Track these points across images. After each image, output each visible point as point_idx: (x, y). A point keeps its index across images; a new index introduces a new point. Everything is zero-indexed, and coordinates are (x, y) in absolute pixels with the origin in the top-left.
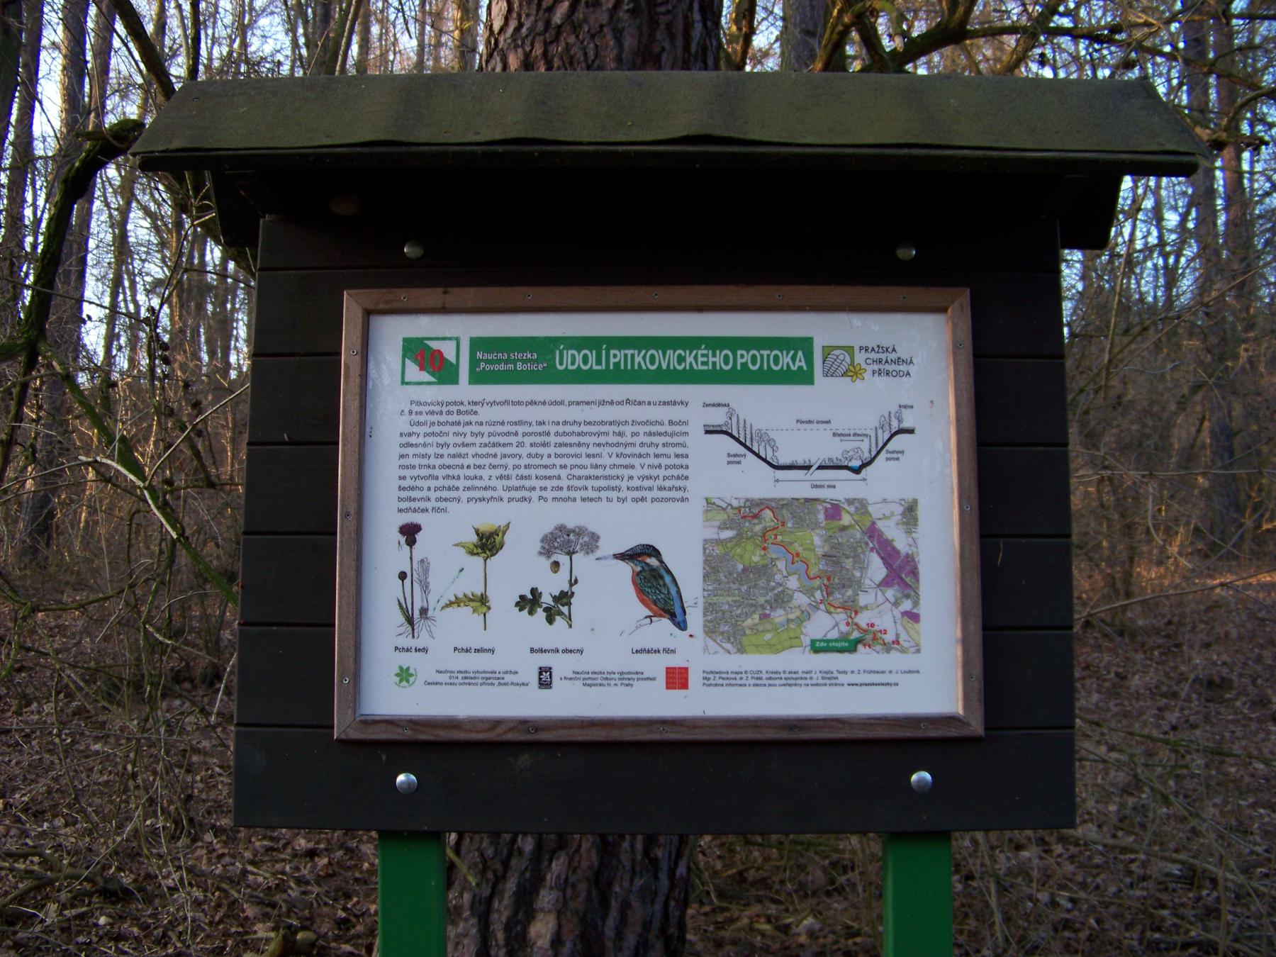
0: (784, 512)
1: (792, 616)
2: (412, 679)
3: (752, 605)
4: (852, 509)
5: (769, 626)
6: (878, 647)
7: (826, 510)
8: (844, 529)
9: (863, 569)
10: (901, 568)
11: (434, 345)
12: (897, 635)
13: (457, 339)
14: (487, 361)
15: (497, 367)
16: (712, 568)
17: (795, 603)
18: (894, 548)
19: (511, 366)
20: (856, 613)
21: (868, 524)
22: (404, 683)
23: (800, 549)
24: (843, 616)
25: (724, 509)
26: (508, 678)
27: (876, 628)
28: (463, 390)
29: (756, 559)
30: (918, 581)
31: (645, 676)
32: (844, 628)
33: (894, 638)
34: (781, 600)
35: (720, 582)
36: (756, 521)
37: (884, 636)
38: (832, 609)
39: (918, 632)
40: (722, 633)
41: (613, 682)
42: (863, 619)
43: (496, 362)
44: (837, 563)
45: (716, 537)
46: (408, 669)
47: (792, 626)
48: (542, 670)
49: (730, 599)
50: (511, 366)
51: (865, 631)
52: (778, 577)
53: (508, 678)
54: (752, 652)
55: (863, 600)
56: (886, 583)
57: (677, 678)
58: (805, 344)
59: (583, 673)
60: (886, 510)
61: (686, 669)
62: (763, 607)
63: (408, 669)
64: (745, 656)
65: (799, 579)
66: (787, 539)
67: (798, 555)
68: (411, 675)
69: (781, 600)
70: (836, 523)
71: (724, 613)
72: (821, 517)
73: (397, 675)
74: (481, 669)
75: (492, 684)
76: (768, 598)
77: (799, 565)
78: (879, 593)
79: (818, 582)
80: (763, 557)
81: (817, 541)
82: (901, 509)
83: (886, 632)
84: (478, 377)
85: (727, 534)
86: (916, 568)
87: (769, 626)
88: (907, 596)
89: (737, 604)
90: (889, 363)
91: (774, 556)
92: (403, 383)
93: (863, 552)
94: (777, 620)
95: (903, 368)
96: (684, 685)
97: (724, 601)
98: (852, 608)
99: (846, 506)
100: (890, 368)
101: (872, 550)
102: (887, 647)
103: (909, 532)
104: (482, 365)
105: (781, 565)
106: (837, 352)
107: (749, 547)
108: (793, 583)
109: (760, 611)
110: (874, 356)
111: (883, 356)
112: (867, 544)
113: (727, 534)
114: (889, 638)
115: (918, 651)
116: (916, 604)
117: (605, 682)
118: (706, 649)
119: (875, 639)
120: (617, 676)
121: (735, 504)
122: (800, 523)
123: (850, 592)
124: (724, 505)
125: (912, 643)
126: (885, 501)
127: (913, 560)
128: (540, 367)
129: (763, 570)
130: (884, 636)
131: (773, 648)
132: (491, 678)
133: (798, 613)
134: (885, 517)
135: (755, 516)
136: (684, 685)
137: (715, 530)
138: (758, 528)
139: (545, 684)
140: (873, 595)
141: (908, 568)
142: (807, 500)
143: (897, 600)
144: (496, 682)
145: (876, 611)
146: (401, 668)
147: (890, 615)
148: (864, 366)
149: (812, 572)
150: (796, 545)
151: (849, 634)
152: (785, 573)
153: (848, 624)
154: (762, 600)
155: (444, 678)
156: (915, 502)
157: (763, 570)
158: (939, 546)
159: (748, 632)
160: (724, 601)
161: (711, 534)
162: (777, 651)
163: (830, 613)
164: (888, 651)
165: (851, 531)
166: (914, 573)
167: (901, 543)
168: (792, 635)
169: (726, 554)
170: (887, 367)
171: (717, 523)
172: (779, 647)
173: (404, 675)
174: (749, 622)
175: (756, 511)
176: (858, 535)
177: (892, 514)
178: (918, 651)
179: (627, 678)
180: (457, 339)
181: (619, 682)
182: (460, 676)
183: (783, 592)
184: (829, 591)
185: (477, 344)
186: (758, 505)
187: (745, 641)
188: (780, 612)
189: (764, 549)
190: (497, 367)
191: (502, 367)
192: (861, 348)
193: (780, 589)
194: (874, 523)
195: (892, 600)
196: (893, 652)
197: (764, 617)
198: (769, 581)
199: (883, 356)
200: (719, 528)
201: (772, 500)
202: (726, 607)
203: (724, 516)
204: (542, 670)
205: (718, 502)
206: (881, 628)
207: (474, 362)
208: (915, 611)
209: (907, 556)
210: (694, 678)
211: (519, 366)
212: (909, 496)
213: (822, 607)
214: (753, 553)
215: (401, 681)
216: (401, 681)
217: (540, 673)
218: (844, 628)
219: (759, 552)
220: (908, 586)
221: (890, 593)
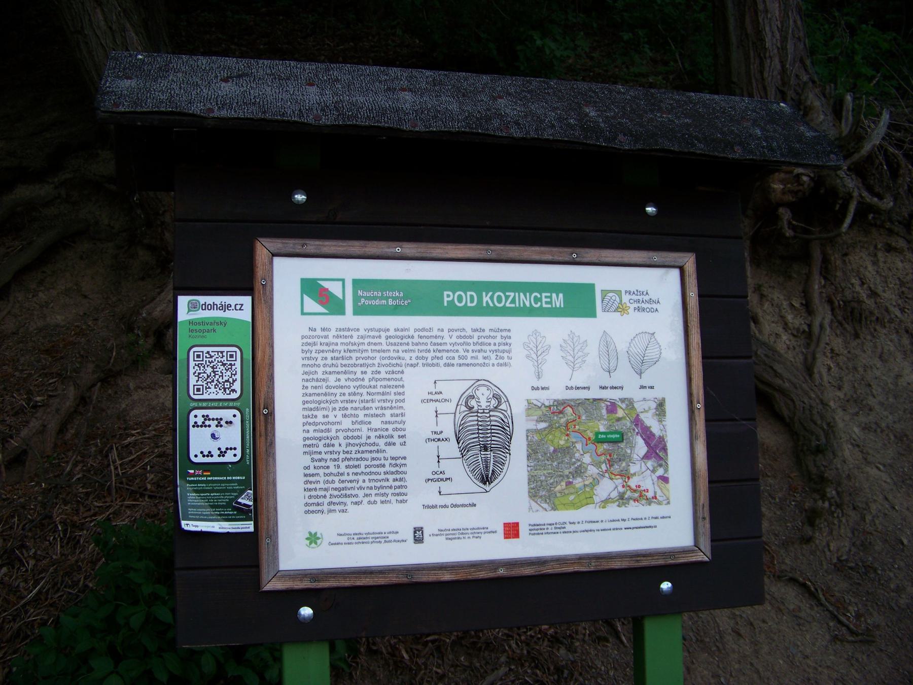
0: (580, 408)
1: (587, 483)
2: (319, 542)
3: (561, 476)
4: (624, 406)
5: (572, 490)
7: (607, 406)
8: (619, 420)
9: (632, 448)
10: (656, 446)
11: (325, 284)
12: (655, 493)
13: (343, 280)
14: (366, 298)
15: (374, 302)
17: (589, 473)
19: (384, 302)
20: (629, 478)
21: (634, 416)
22: (313, 545)
24: (620, 481)
25: (540, 408)
26: (392, 537)
28: (349, 319)
29: (562, 442)
30: (667, 454)
31: (489, 530)
32: (621, 489)
34: (579, 471)
36: (561, 415)
39: (668, 490)
40: (541, 497)
41: (467, 536)
42: (633, 483)
43: (374, 299)
45: (535, 427)
46: (316, 533)
48: (416, 530)
49: (545, 472)
50: (384, 302)
51: (635, 491)
52: (577, 455)
53: (392, 537)
55: (633, 469)
56: (646, 457)
57: (512, 531)
58: (589, 289)
59: (445, 530)
60: (646, 405)
61: (517, 524)
62: (568, 477)
63: (316, 533)
64: (557, 512)
65: (591, 456)
68: (319, 538)
69: (579, 471)
70: (614, 416)
71: (542, 482)
72: (604, 411)
73: (307, 539)
74: (371, 531)
75: (380, 542)
76: (571, 470)
79: (603, 458)
82: (654, 405)
84: (359, 310)
85: (543, 425)
87: (572, 490)
88: (661, 466)
89: (550, 475)
90: (646, 303)
91: (574, 440)
92: (303, 313)
94: (577, 486)
95: (655, 306)
96: (517, 536)
97: (541, 474)
98: (626, 475)
99: (620, 404)
100: (644, 305)
102: (649, 501)
103: (660, 421)
104: (363, 300)
105: (579, 446)
106: (610, 294)
107: (557, 434)
108: (587, 459)
109: (566, 480)
110: (635, 297)
111: (640, 298)
113: (543, 425)
114: (650, 495)
115: (669, 503)
116: (666, 471)
117: (461, 536)
118: (530, 508)
119: (641, 496)
120: (469, 531)
121: (547, 404)
122: (590, 418)
123: (624, 464)
124: (539, 405)
126: (644, 400)
128: (406, 302)
129: (567, 451)
131: (575, 506)
132: (379, 538)
133: (591, 480)
134: (645, 411)
135: (561, 412)
136: (517, 536)
137: (534, 423)
138: (563, 421)
139: (418, 540)
140: (639, 466)
141: (661, 446)
142: (595, 400)
144: (383, 540)
146: (310, 533)
148: (628, 304)
151: (624, 493)
153: (623, 486)
155: (344, 539)
156: (664, 399)
157: (567, 451)
158: (677, 431)
159: (558, 495)
161: (532, 425)
163: (612, 479)
165: (624, 421)
166: (664, 449)
167: (656, 429)
168: (588, 496)
169: (542, 440)
170: (644, 305)
171: (535, 418)
172: (579, 504)
173: (313, 539)
174: (559, 488)
175: (561, 408)
176: (628, 424)
177: (650, 408)
178: (669, 503)
179: (477, 532)
180: (343, 280)
181: (471, 536)
182: (356, 537)
184: (611, 463)
185: (358, 284)
187: (557, 502)
188: (579, 480)
189: (567, 435)
190: (374, 302)
191: (377, 302)
192: (626, 292)
193: (579, 463)
194: (638, 415)
195: (651, 468)
197: (569, 483)
198: (571, 458)
199: (640, 298)
200: (537, 421)
201: (571, 400)
202: (543, 478)
203: (539, 413)
204: (416, 530)
205: (535, 402)
207: (356, 299)
210: (523, 530)
211: (390, 302)
212: (660, 396)
213: (607, 475)
214: (560, 439)
215: (311, 543)
216: (311, 543)
217: (415, 532)
218: (621, 489)
220: (661, 459)
221: (650, 464)
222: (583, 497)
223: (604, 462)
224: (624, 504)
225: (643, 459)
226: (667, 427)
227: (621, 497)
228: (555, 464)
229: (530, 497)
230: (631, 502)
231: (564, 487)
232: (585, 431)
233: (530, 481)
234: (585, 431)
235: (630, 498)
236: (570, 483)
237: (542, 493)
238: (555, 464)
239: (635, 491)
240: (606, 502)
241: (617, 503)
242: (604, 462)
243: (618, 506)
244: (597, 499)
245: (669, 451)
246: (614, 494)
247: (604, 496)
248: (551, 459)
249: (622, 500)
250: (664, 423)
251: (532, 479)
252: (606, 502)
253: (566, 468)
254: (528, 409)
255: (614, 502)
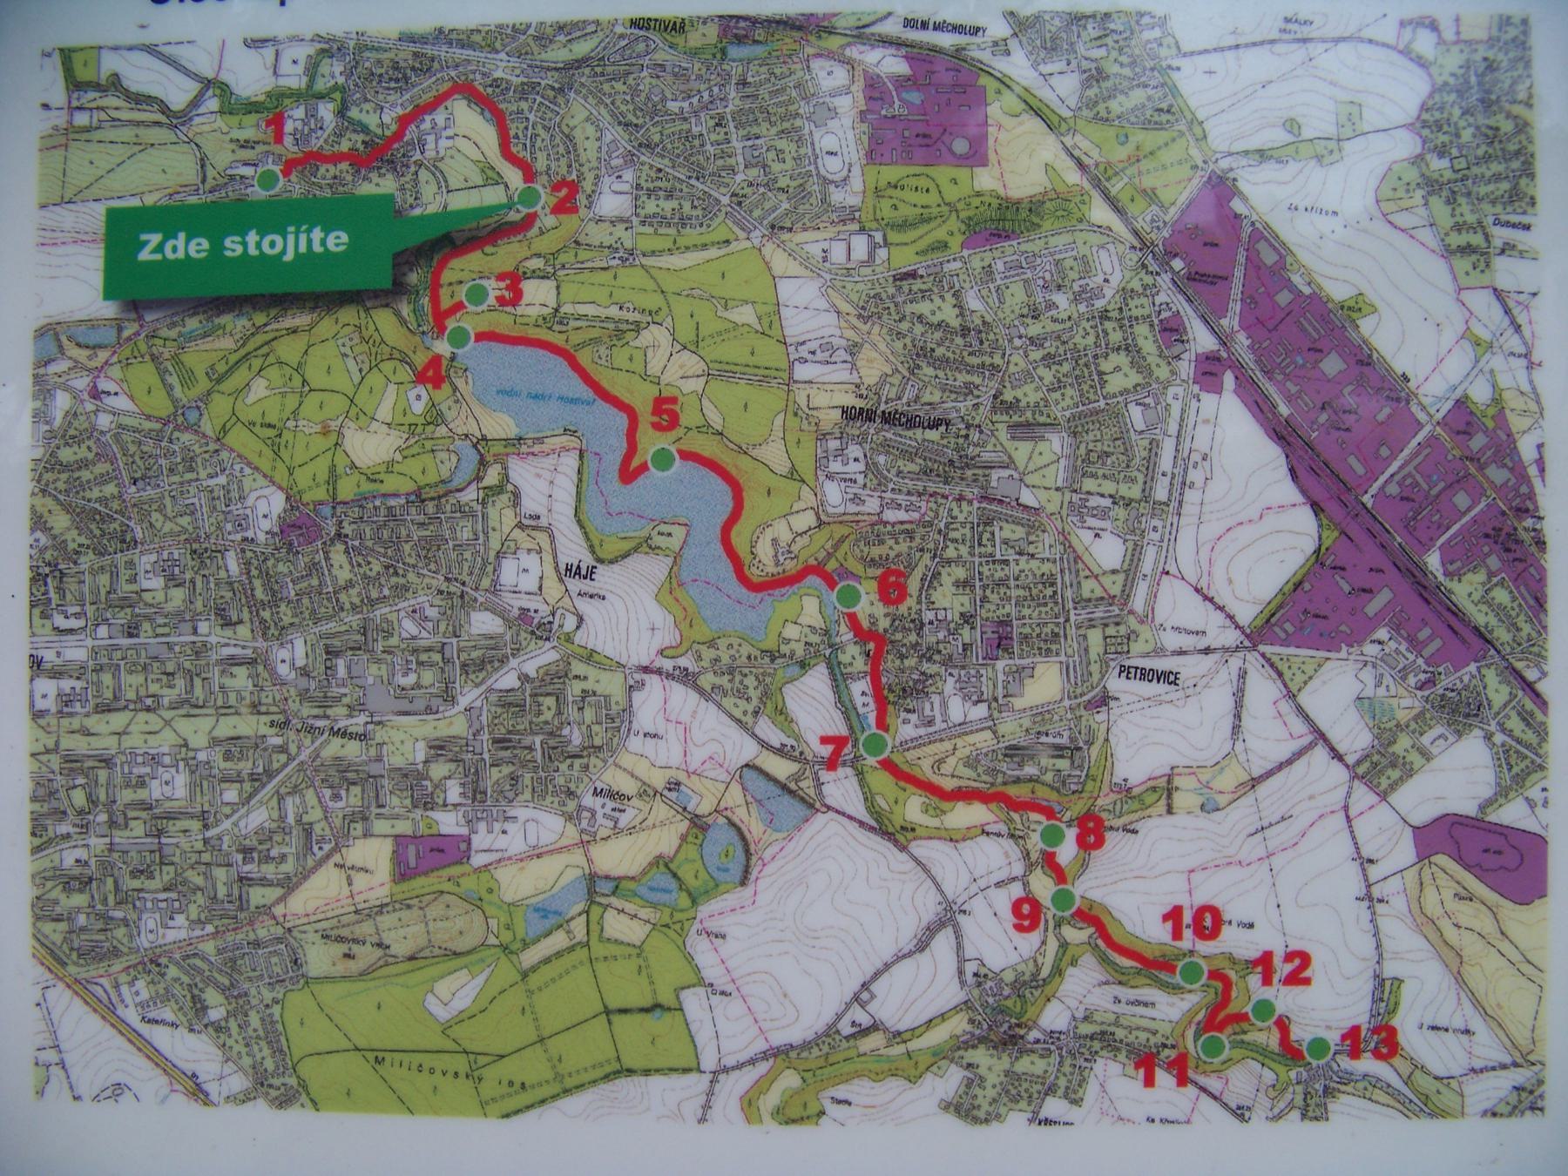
0: (578, 112)
3: (344, 775)
5: (461, 927)
6: (1243, 1080)
7: (875, 89)
8: (1001, 223)
9: (1148, 510)
12: (1385, 991)
16: (83, 516)
17: (645, 758)
18: (1363, 360)
20: (1092, 833)
23: (681, 374)
24: (994, 857)
25: (177, 119)
27: (1233, 941)
29: (371, 446)
32: (999, 946)
33: (1358, 1012)
34: (545, 738)
35: (132, 614)
37: (1285, 999)
38: (914, 808)
39: (1529, 968)
40: (152, 963)
42: (1135, 884)
44: (959, 466)
47: (618, 926)
49: (198, 730)
51: (1155, 966)
52: (522, 575)
54: (349, 1098)
55: (1145, 737)
56: (1306, 617)
62: (413, 782)
64: (297, 1116)
65: (673, 586)
66: (589, 299)
67: (666, 411)
70: (952, 182)
71: (160, 819)
72: (839, 140)
76: (454, 724)
77: (681, 492)
78: (1262, 690)
79: (808, 609)
80: (421, 432)
81: (808, 310)
82: (1399, 93)
83: (1299, 969)
86: (1526, 507)
88: (1462, 712)
91: (499, 425)
93: (1148, 390)
94: (518, 884)
97: (165, 745)
98: (1060, 801)
99: (1018, 66)
101: (1209, 371)
102: (1311, 1077)
103: (1471, 252)
105: (546, 485)
108: (628, 617)
112: (1172, 331)
114: (1325, 1008)
115: (1528, 1100)
116: (1521, 764)
119: (1219, 1018)
121: (250, 77)
123: (1045, 684)
124: (178, 92)
125: (1487, 1047)
127: (1504, 449)
129: (422, 527)
130: (1285, 999)
133: (665, 839)
134: (1295, 146)
140: (1219, 700)
141: (1468, 508)
142: (738, 29)
143: (1385, 736)
145: (1241, 815)
147: (1331, 847)
149: (776, 534)
150: (656, 335)
151: (1034, 984)
152: (573, 550)
153: (1027, 914)
154: (406, 742)
159: (319, 958)
160: (165, 745)
162: (520, 1100)
164: (1313, 1108)
165: (1052, 242)
166: (1513, 544)
167: (1421, 336)
168: (626, 989)
169: (179, 419)
172: (532, 1067)
174: (322, 891)
175: (380, 117)
176: (1112, 269)
177: (1350, 128)
178: (1528, 1100)
183: (555, 678)
184: (891, 668)
186: (400, 77)
187: (306, 1026)
188: (539, 823)
189: (433, 374)
193: (539, 659)
194: (1222, 188)
195: (1354, 737)
196: (1344, 1106)
197: (426, 857)
198: (459, 602)
202: (174, 787)
205: (143, 75)
206: (1266, 939)
208: (1512, 814)
209: (1463, 418)
213: (841, 788)
214: (357, 412)
219: (397, 397)
221: (1339, 689)
222: (569, 996)
223: (823, 651)
224: (1023, 1095)
225: (1257, 635)
226: (1544, 321)
227: (1000, 1019)
228: (294, 653)
229: (52, 957)
230: (1112, 1078)
231: (377, 882)
232: (620, 332)
233: (48, 816)
234: (620, 332)
235: (1103, 1039)
236: (445, 852)
237: (167, 930)
238: (294, 653)
239: (1155, 966)
240: (816, 1070)
241: (950, 1081)
242: (823, 651)
243: (963, 1109)
244: (723, 1030)
245: (1562, 569)
246: (924, 992)
247: (809, 1008)
248: (259, 603)
249: (1005, 1047)
250: (1506, 272)
251: (68, 793)
252: (816, 1070)
253: (408, 703)
254: (63, 139)
255: (911, 1070)
